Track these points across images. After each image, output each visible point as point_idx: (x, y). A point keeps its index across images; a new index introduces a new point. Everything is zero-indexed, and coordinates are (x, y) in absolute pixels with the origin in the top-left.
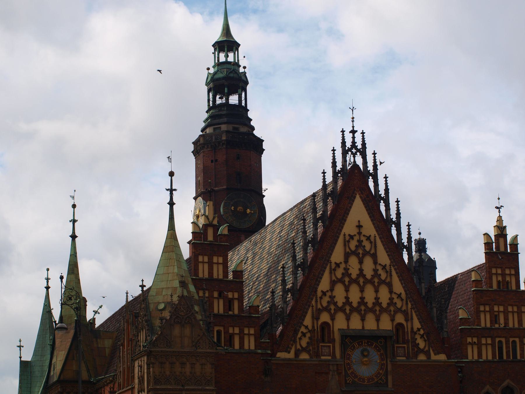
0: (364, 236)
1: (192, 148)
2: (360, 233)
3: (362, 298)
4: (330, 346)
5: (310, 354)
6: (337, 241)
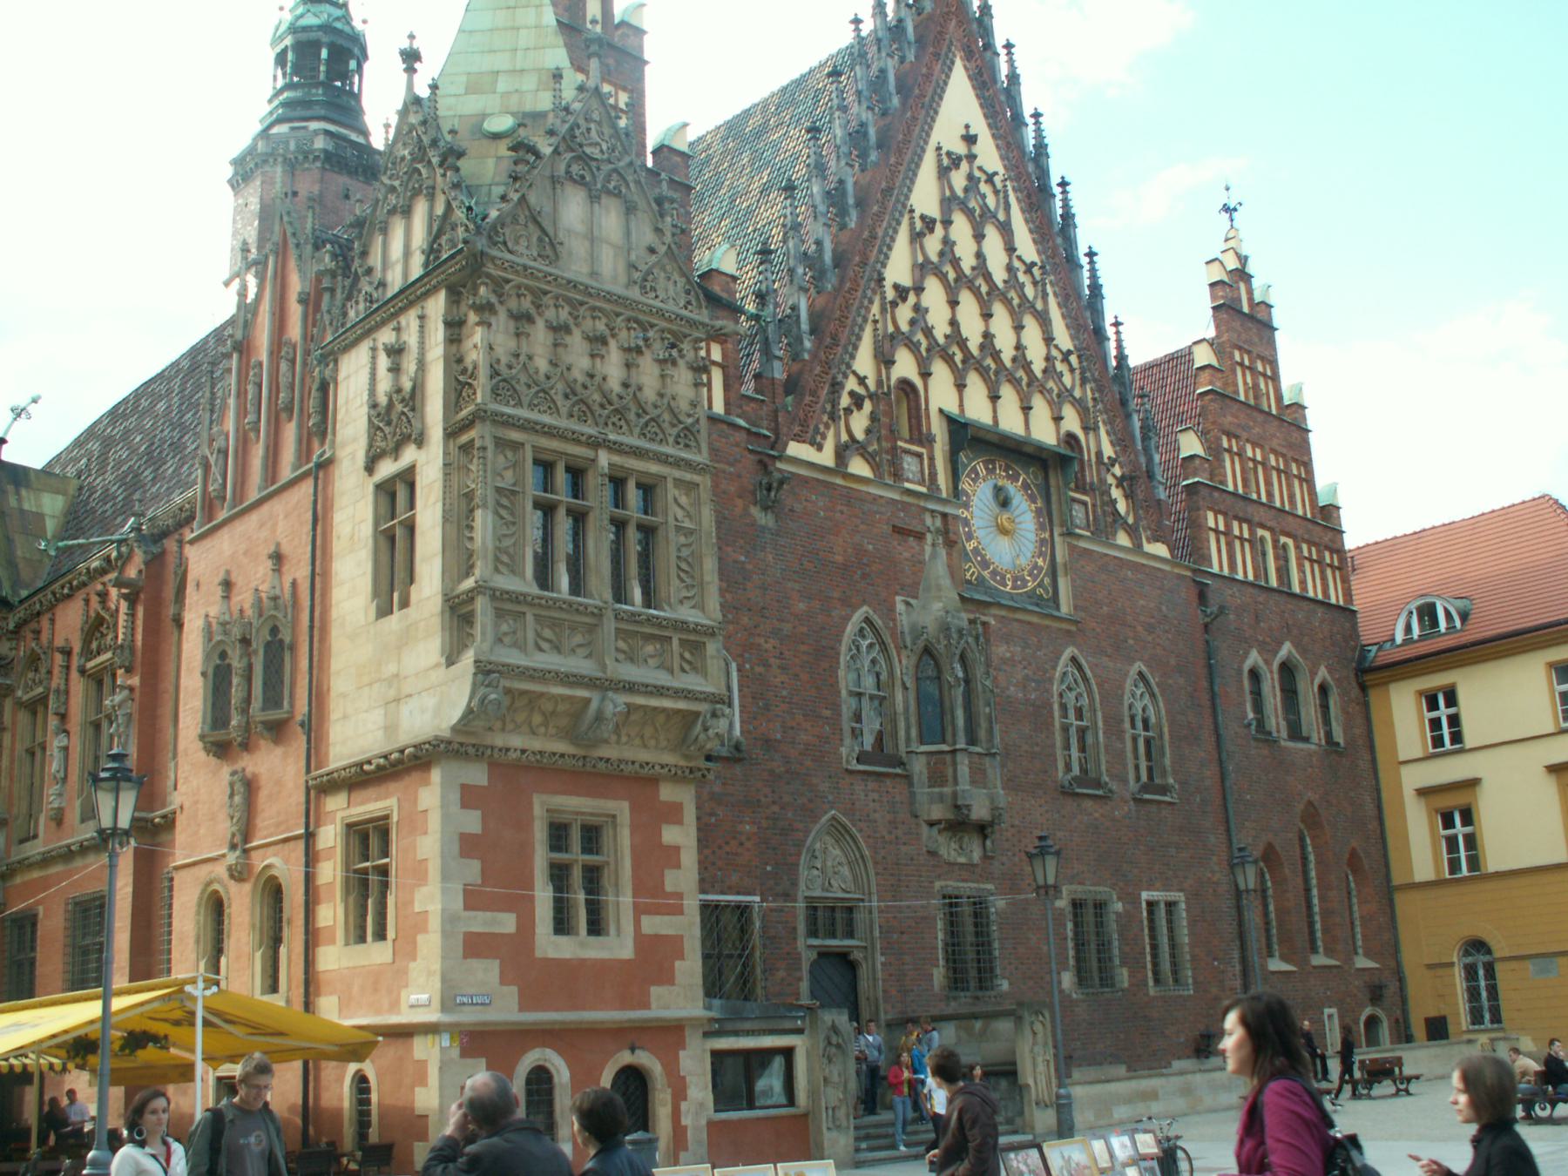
0: (980, 168)
1: (229, 171)
2: (971, 157)
3: (987, 336)
4: (919, 456)
5: (875, 467)
6: (921, 158)
